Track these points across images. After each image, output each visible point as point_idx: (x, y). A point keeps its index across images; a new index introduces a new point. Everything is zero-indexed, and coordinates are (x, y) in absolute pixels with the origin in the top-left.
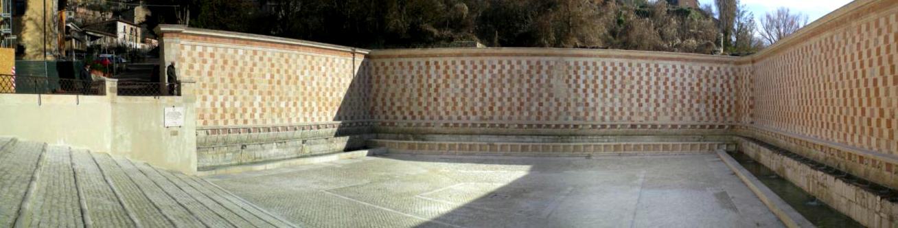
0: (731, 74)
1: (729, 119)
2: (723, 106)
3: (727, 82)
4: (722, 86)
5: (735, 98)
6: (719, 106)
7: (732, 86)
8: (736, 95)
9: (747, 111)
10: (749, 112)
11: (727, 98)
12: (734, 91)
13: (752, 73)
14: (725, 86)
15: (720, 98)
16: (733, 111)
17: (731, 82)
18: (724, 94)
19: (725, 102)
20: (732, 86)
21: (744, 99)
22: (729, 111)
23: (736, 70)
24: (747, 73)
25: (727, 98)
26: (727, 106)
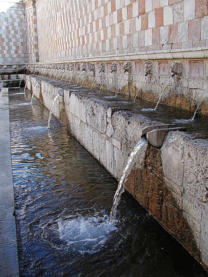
0: (15, 16)
1: (17, 60)
2: (10, 48)
3: (12, 24)
4: (7, 28)
5: (21, 40)
6: (7, 48)
7: (18, 28)
8: (22, 37)
9: (32, 52)
10: (34, 51)
11: (14, 40)
12: (20, 33)
13: (35, 13)
14: (10, 28)
15: (6, 40)
16: (20, 52)
17: (16, 24)
18: (11, 36)
19: (11, 44)
20: (18, 28)
21: (30, 40)
22: (16, 52)
23: (20, 12)
24: (30, 15)
25: (14, 40)
26: (14, 48)
